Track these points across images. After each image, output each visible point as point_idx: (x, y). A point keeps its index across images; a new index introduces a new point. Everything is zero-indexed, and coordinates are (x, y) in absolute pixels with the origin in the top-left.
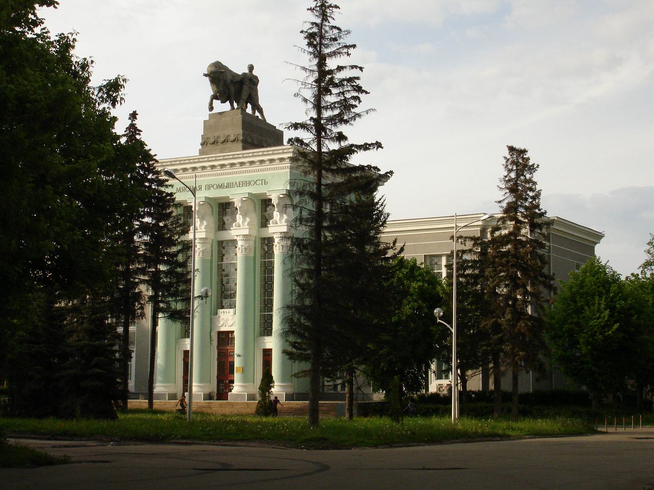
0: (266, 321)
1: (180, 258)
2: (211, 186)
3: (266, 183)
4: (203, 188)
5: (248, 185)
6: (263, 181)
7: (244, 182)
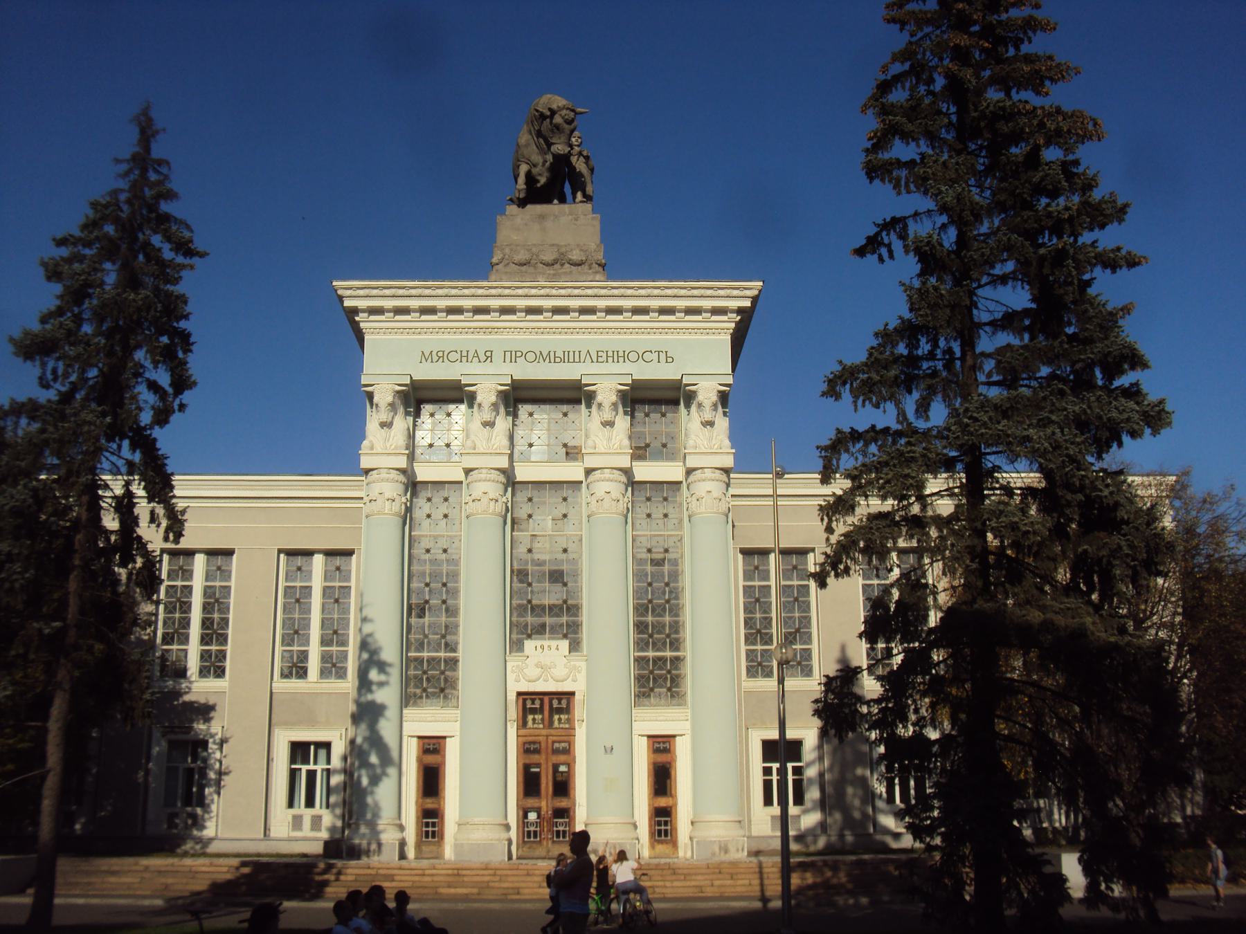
0: (799, 663)
1: (952, 420)
2: (519, 354)
3: (669, 359)
4: (498, 356)
5: (621, 359)
6: (663, 356)
7: (610, 354)
